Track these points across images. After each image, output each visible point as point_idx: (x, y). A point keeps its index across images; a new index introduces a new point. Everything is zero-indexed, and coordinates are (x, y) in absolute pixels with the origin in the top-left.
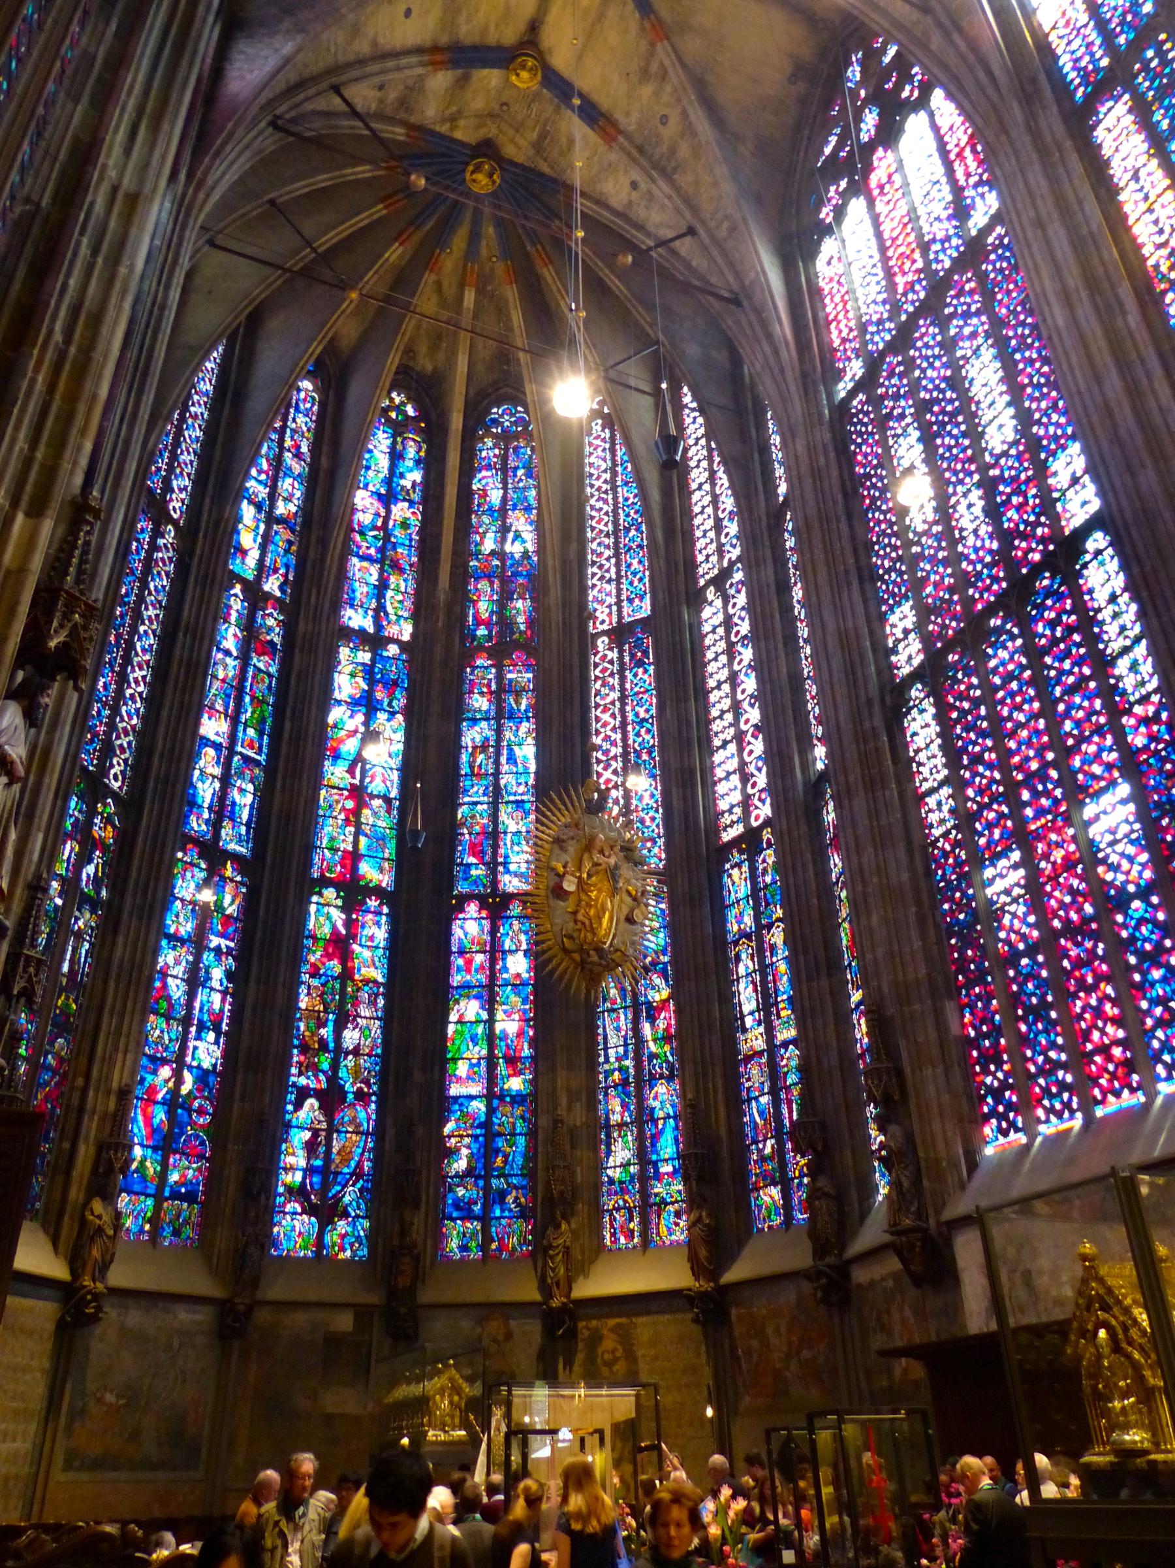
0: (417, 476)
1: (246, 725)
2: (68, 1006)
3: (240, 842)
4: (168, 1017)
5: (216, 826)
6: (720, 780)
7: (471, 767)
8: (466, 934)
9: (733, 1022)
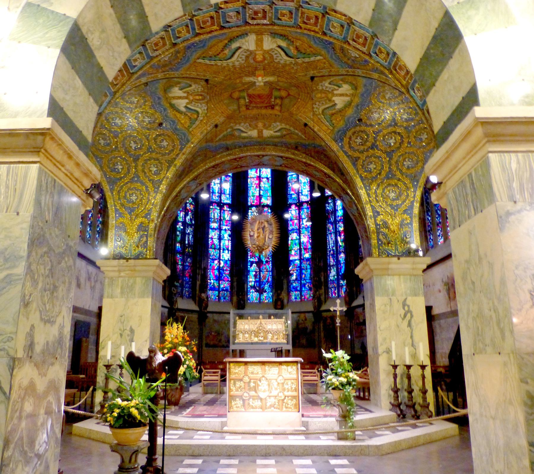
2: (189, 251)
3: (227, 199)
4: (215, 249)
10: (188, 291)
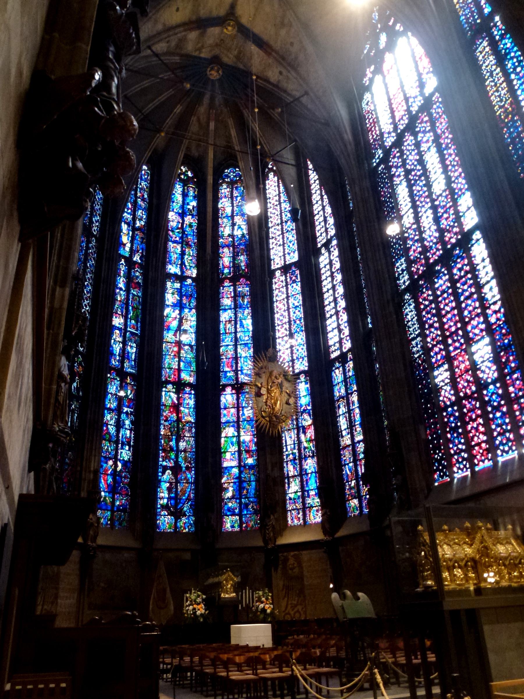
0: (194, 203)
3: (132, 368)
4: (110, 441)
5: (122, 362)
6: (330, 332)
7: (225, 330)
8: (227, 401)
9: (337, 434)
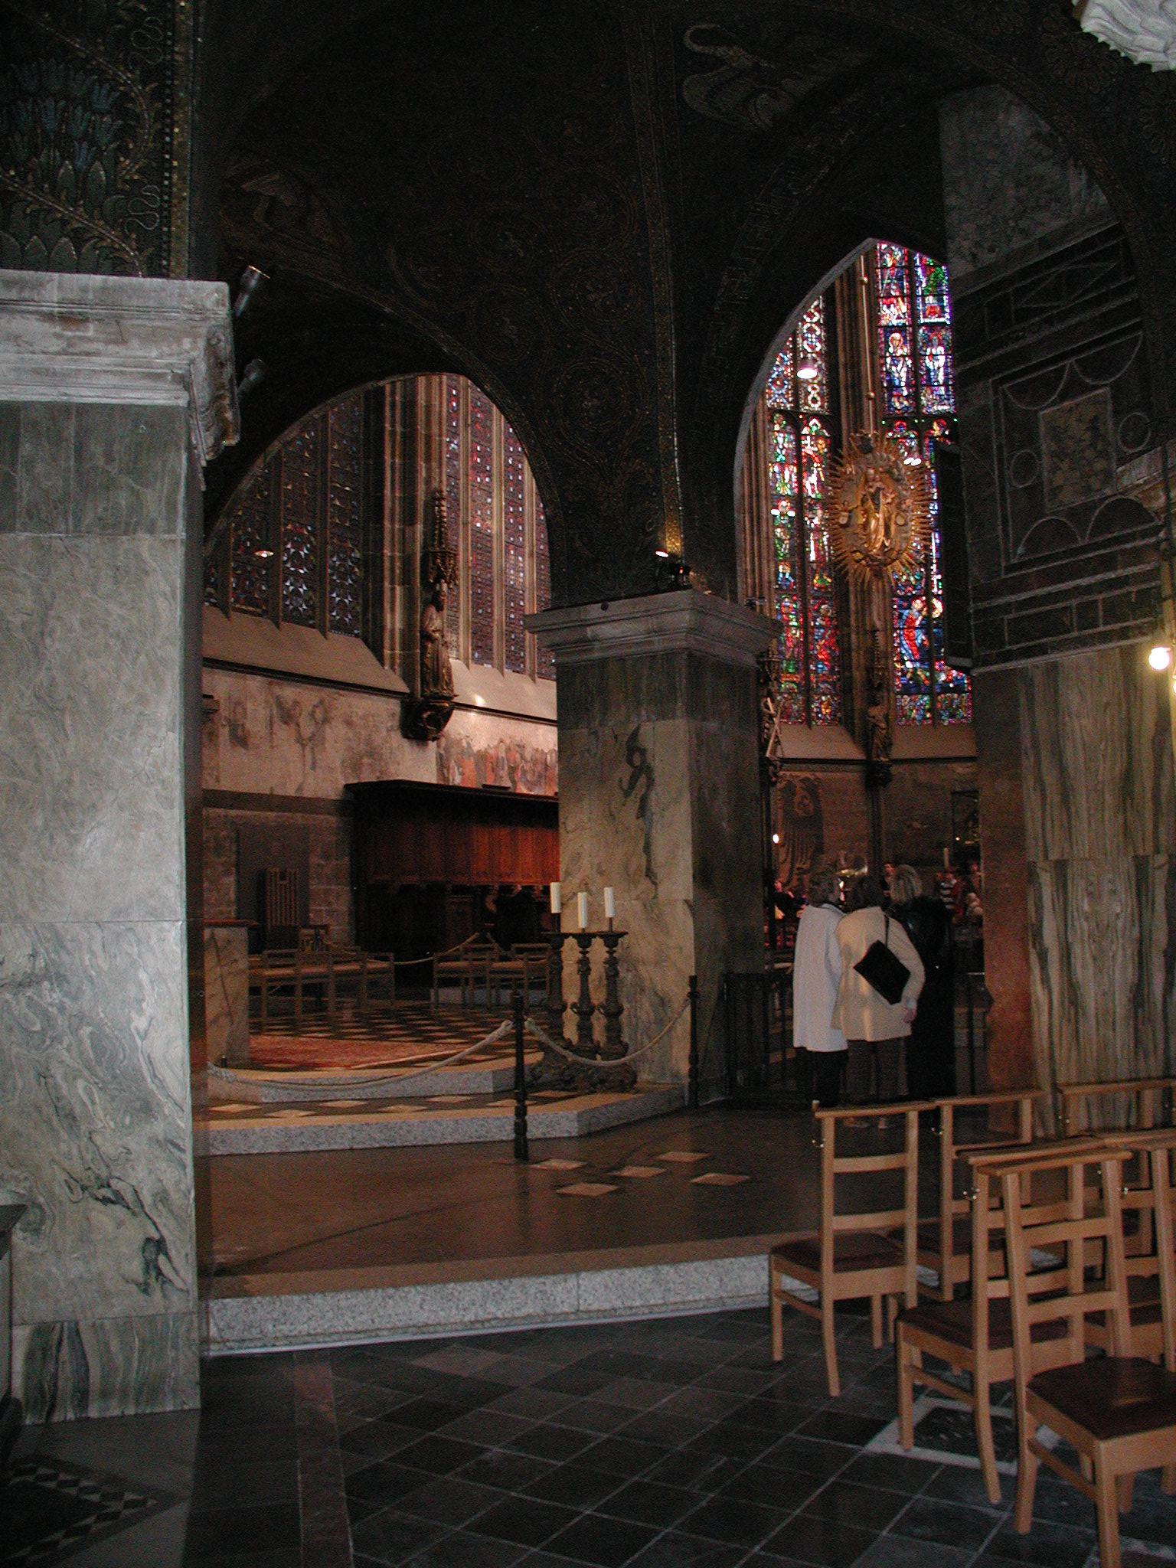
1: (923, 296)
2: (824, 581)
3: (941, 403)
5: (915, 397)
10: (829, 704)
